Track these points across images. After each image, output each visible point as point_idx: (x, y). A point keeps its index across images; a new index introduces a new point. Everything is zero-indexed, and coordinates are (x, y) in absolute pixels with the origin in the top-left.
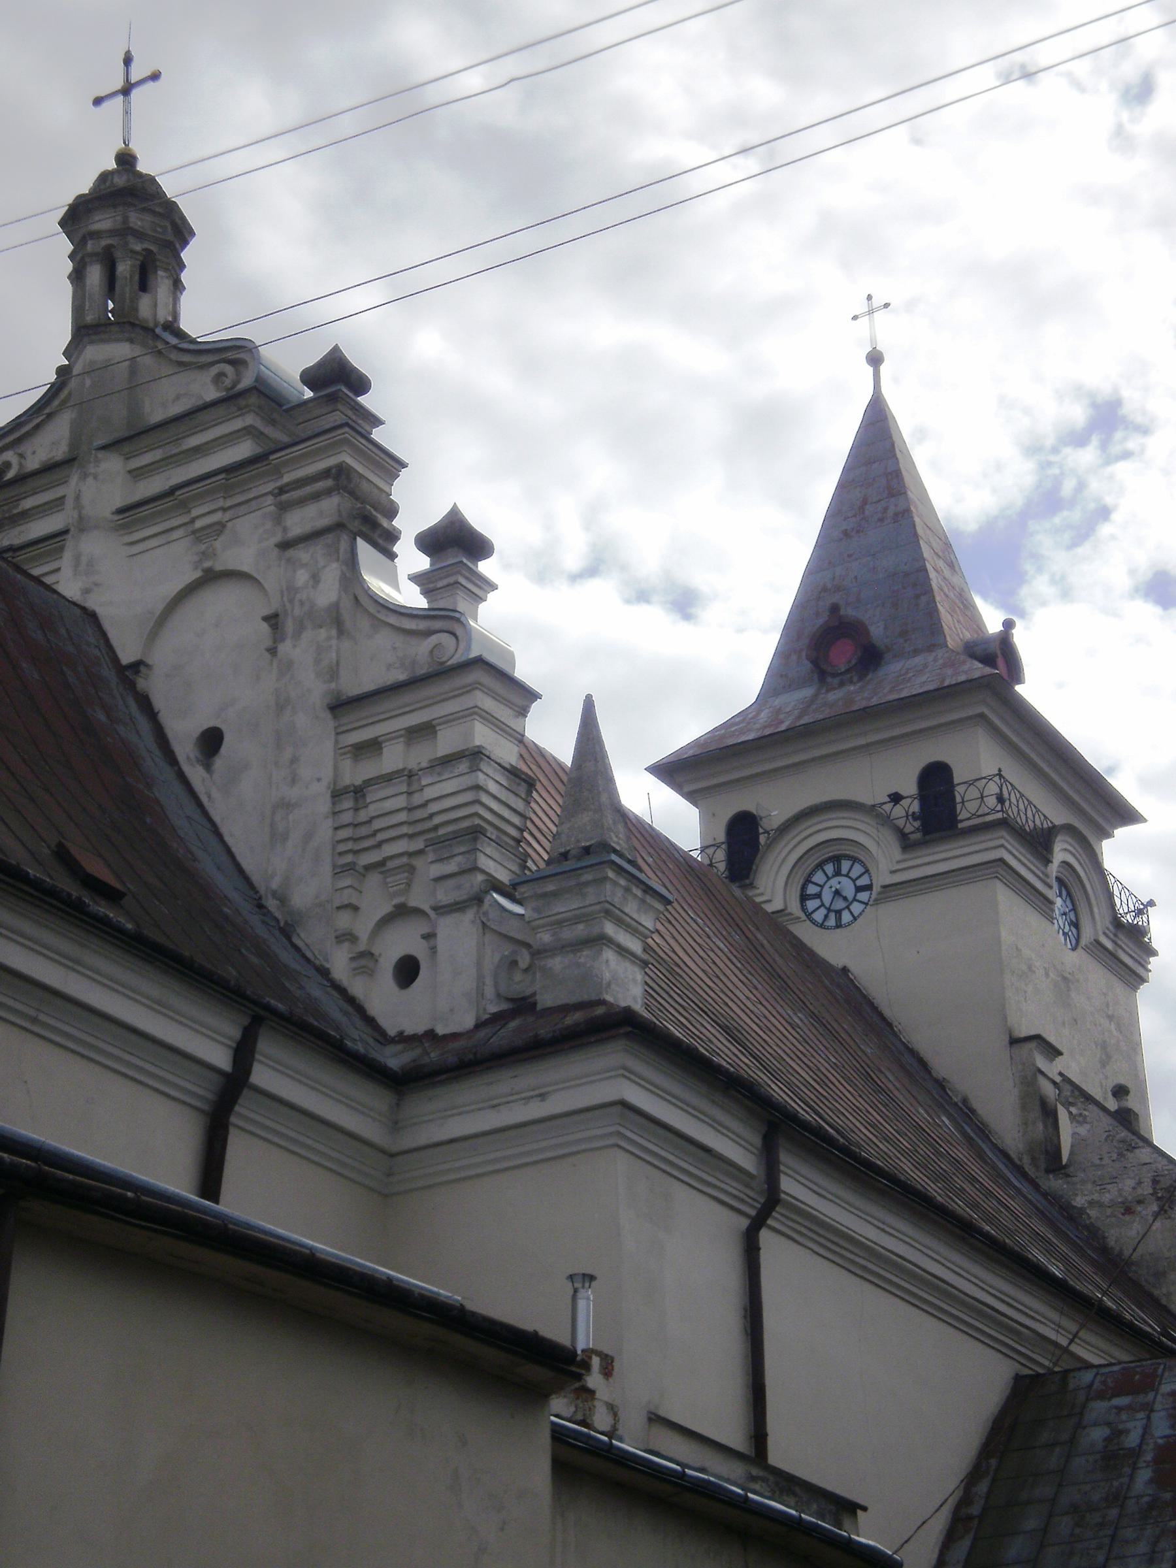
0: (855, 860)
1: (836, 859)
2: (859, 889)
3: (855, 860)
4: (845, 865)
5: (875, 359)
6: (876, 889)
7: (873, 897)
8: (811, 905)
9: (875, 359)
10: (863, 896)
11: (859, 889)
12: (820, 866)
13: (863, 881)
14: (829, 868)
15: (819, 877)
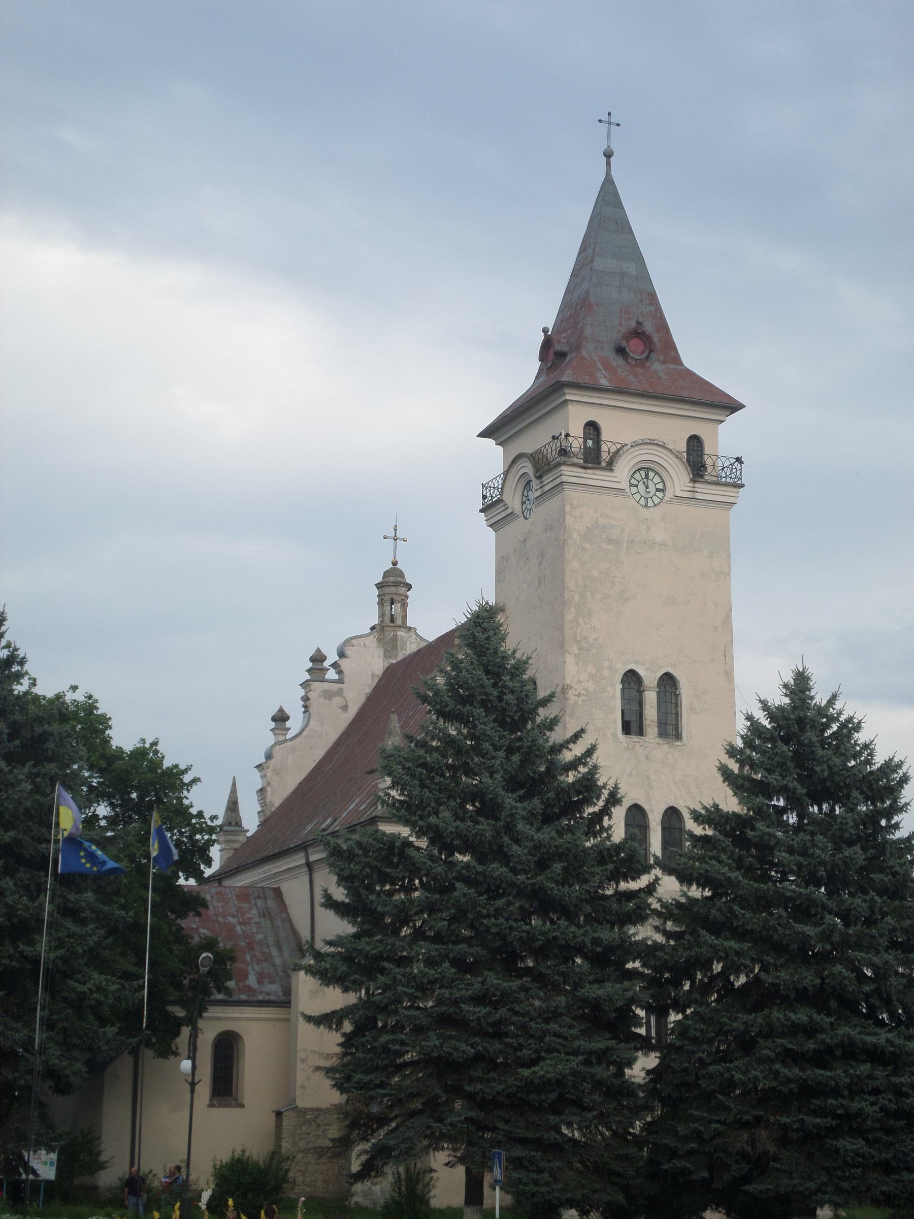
0: (656, 473)
1: (647, 470)
2: (658, 490)
3: (656, 473)
4: (651, 474)
5: (608, 155)
6: (669, 494)
7: (666, 499)
8: (634, 490)
9: (608, 155)
10: (660, 494)
11: (658, 490)
12: (639, 470)
13: (660, 486)
14: (643, 473)
15: (637, 476)
